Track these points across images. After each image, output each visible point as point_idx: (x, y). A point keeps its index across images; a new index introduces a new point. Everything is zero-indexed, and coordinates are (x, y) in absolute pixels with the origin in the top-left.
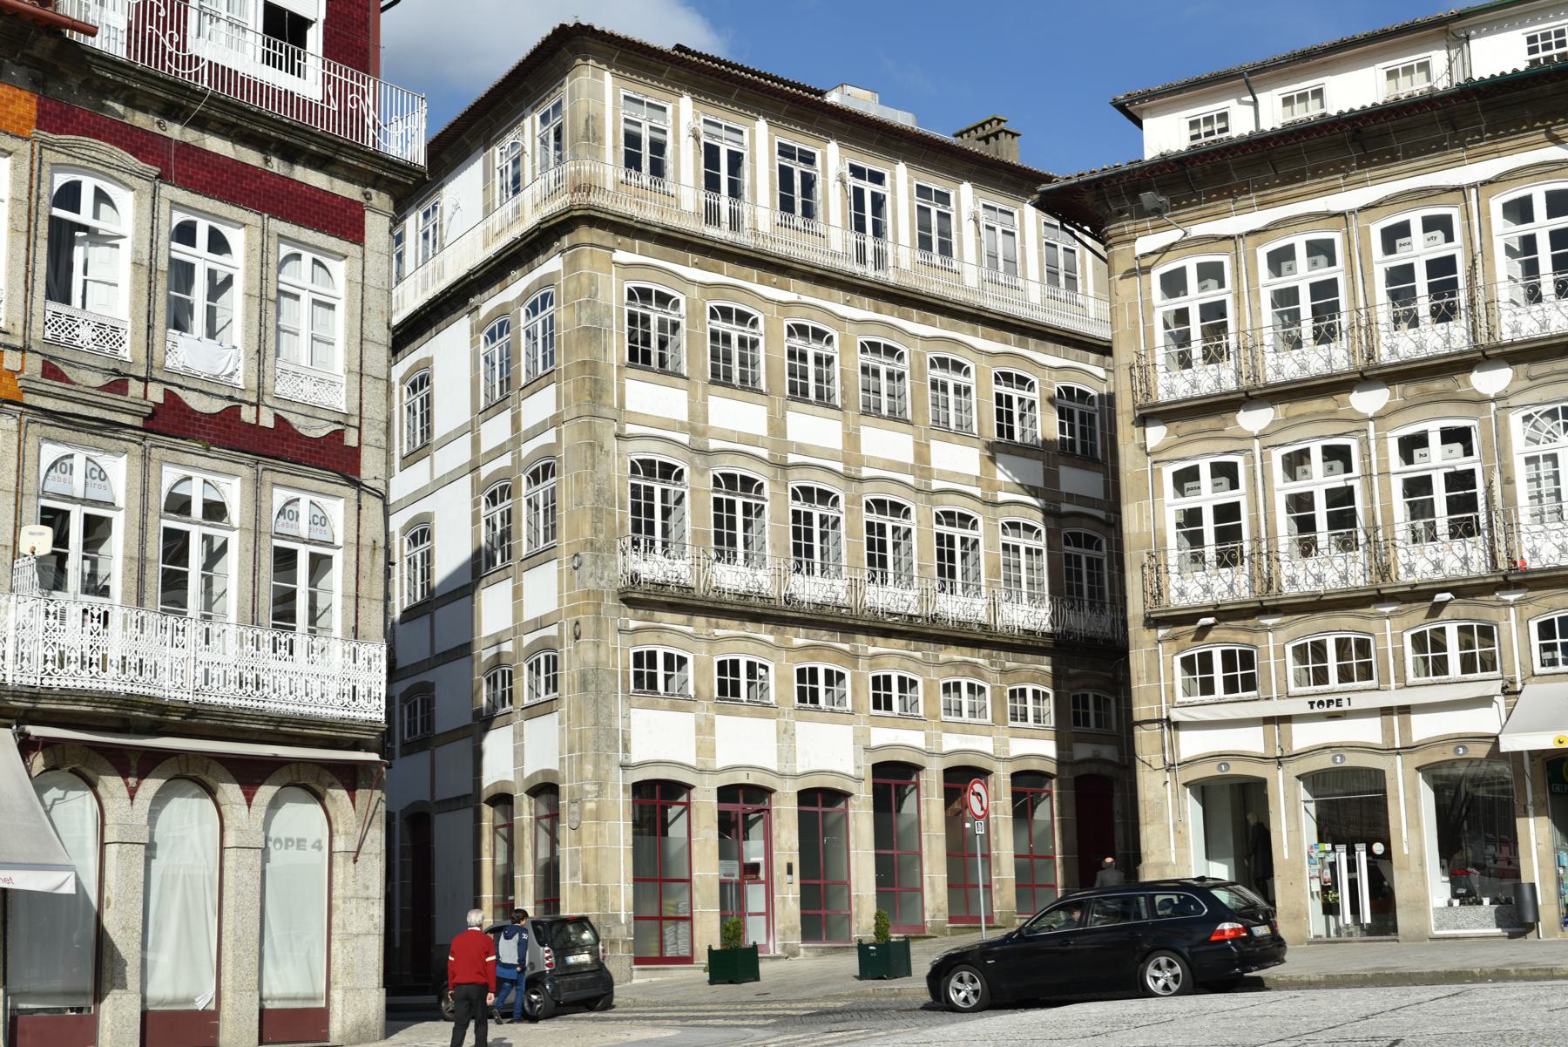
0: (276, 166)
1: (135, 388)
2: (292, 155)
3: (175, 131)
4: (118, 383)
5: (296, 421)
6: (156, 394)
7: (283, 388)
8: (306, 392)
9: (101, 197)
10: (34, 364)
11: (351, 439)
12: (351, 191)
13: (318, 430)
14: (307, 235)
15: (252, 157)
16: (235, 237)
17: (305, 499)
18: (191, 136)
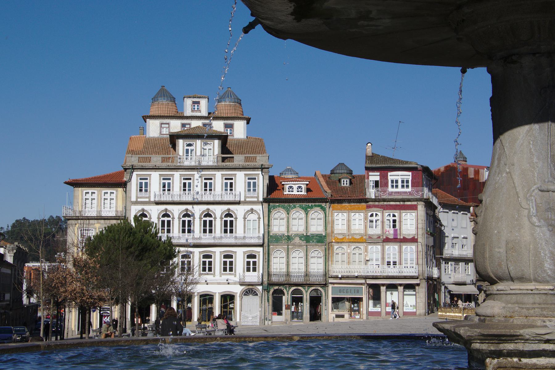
0: (402, 203)
1: (381, 237)
2: (404, 201)
3: (385, 203)
4: (379, 237)
5: (407, 237)
6: (385, 237)
7: (404, 233)
8: (409, 232)
9: (376, 215)
10: (368, 237)
11: (416, 237)
12: (415, 203)
13: (411, 237)
14: (408, 211)
15: (398, 203)
16: (396, 214)
17: (409, 247)
18: (388, 203)
